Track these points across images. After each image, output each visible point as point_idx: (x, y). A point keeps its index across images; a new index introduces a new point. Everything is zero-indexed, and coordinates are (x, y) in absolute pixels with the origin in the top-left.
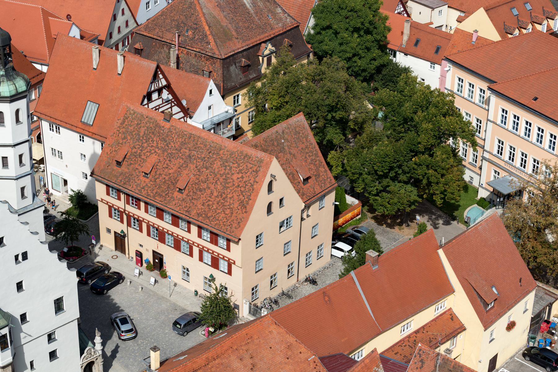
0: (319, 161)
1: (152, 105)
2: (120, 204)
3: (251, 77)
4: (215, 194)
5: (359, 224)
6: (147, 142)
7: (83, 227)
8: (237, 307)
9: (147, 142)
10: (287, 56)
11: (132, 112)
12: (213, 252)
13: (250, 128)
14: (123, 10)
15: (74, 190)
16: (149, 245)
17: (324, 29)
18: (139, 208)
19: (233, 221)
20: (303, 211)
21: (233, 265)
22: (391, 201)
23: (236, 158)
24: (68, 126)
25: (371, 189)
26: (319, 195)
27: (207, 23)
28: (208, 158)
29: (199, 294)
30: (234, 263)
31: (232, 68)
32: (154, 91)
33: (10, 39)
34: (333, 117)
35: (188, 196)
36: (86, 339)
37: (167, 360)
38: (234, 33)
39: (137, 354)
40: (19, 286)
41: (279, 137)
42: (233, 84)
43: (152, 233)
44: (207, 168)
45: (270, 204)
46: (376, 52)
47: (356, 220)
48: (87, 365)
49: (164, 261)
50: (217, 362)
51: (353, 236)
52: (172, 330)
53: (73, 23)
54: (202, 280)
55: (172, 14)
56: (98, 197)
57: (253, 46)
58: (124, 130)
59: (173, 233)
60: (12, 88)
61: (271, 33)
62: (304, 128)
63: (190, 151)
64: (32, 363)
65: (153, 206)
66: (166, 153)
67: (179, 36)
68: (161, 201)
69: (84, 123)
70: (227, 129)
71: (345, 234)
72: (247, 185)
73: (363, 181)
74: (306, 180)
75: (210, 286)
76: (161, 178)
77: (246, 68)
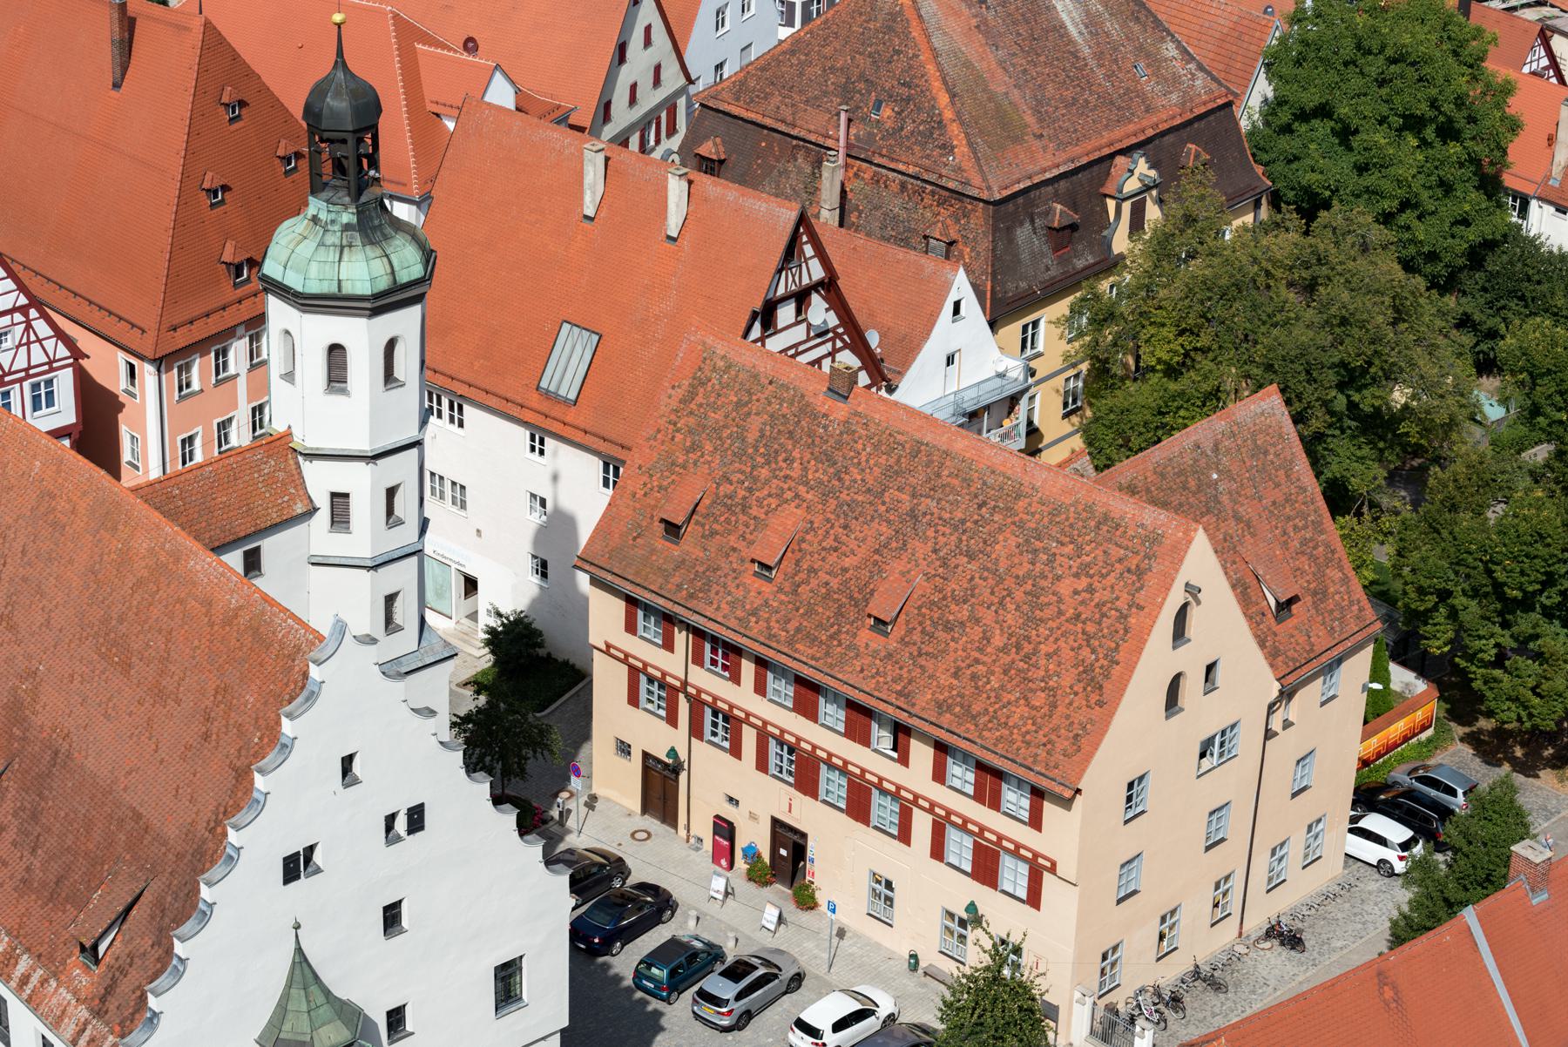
0: (1327, 546)
1: (775, 344)
2: (673, 662)
3: (1080, 264)
4: (998, 640)
5: (1429, 757)
6: (768, 463)
7: (541, 732)
8: (1052, 1012)
10: (1202, 198)
11: (721, 364)
12: (982, 829)
13: (1070, 429)
14: (648, 29)
15: (503, 611)
17: (1303, 116)
18: (736, 678)
19: (1055, 730)
20: (1271, 708)
21: (1047, 876)
22: (1545, 686)
23: (1071, 526)
24: (493, 402)
25: (1478, 644)
26: (1323, 658)
27: (945, 83)
28: (976, 522)
29: (923, 964)
30: (1053, 869)
31: (1023, 233)
32: (784, 299)
33: (378, 110)
34: (1352, 406)
35: (907, 644)
38: (1030, 119)
40: (392, 917)
41: (1203, 462)
42: (1023, 285)
43: (773, 760)
44: (971, 557)
45: (1176, 681)
46: (1471, 199)
47: (1420, 743)
49: (809, 854)
51: (1410, 794)
53: (498, 67)
54: (938, 920)
55: (827, 51)
56: (596, 638)
57: (1090, 164)
58: (692, 421)
59: (846, 762)
60: (379, 267)
61: (1145, 123)
62: (1281, 436)
63: (914, 496)
65: (782, 672)
66: (833, 503)
67: (850, 120)
68: (813, 658)
70: (1001, 431)
71: (1386, 787)
72: (1104, 615)
73: (1453, 614)
74: (1285, 606)
75: (962, 938)
76: (814, 582)
77: (1063, 236)
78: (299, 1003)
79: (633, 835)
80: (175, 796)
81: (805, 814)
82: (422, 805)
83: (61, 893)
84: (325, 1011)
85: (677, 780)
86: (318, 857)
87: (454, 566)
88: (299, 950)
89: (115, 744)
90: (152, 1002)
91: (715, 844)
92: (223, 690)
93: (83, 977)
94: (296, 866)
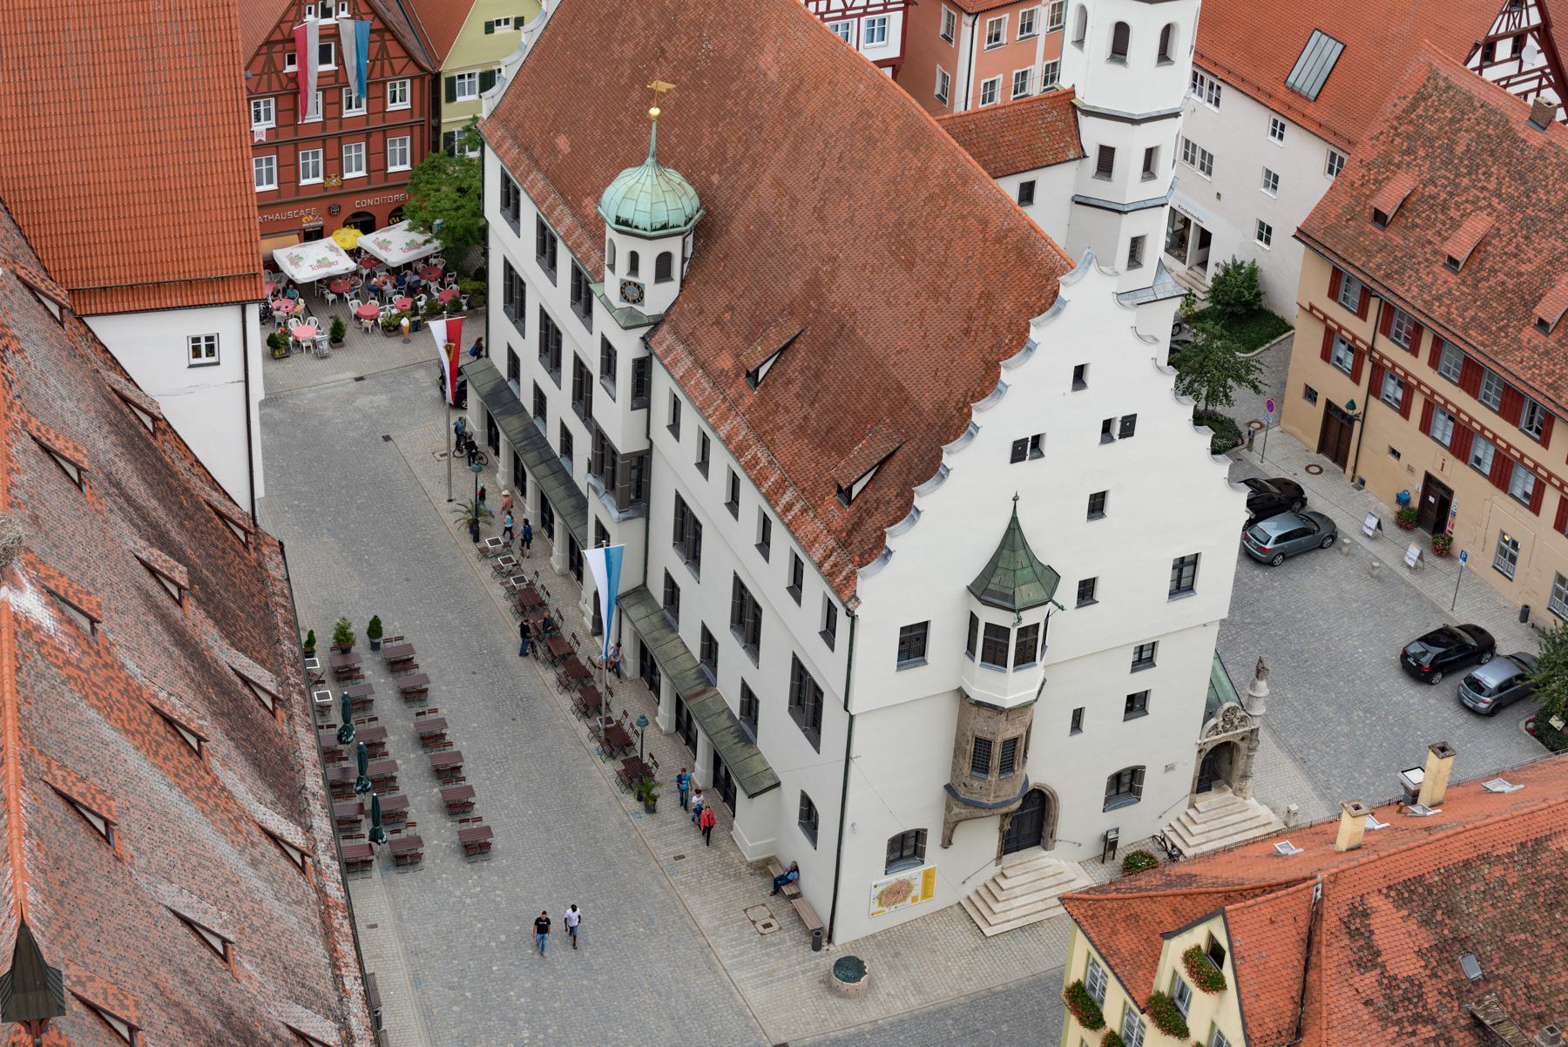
1: (1491, 74)
2: (1363, 330)
6: (1470, 174)
9: (1470, 174)
11: (1442, 84)
40: (1097, 505)
49: (1453, 508)
54: (1549, 583)
59: (1496, 437)
64: (1078, 715)
68: (1482, 344)
69: (1292, 90)
76: (1492, 281)
81: (1455, 475)
83: (831, 441)
86: (1047, 446)
87: (1193, 221)
88: (1014, 519)
89: (893, 325)
90: (889, 542)
92: (987, 296)
93: (839, 515)
94: (1026, 449)
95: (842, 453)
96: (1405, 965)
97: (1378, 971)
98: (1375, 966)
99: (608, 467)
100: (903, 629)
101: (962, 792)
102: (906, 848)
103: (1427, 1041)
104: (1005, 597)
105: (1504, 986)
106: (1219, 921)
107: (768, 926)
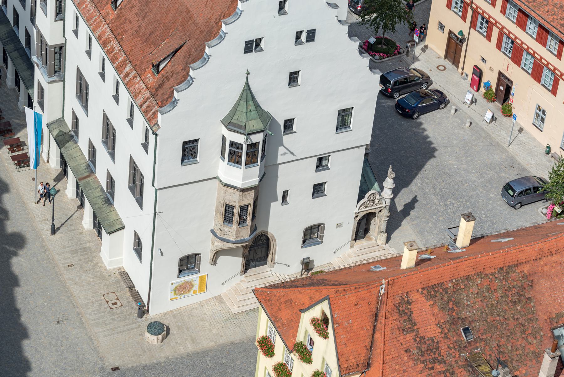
16: (496, 63)
29: (552, 152)
36: (372, 178)
37: (482, 237)
39: (441, 219)
40: (293, 78)
43: (504, 45)
48: (364, 216)
49: (512, 91)
50: (554, 258)
52: (500, 196)
59: (534, 52)
78: (243, 108)
79: (438, 67)
80: (205, 5)
82: (315, 30)
83: (150, 40)
84: (254, 114)
85: (462, 47)
86: (262, 44)
88: (247, 84)
90: (176, 94)
91: (473, 77)
93: (151, 78)
94: (252, 46)
95: (157, 47)
96: (431, 331)
97: (414, 334)
98: (413, 331)
99: (44, 53)
100: (184, 143)
101: (218, 233)
102: (188, 263)
103: (440, 373)
104: (240, 127)
105: (486, 345)
106: (326, 303)
107: (116, 304)
